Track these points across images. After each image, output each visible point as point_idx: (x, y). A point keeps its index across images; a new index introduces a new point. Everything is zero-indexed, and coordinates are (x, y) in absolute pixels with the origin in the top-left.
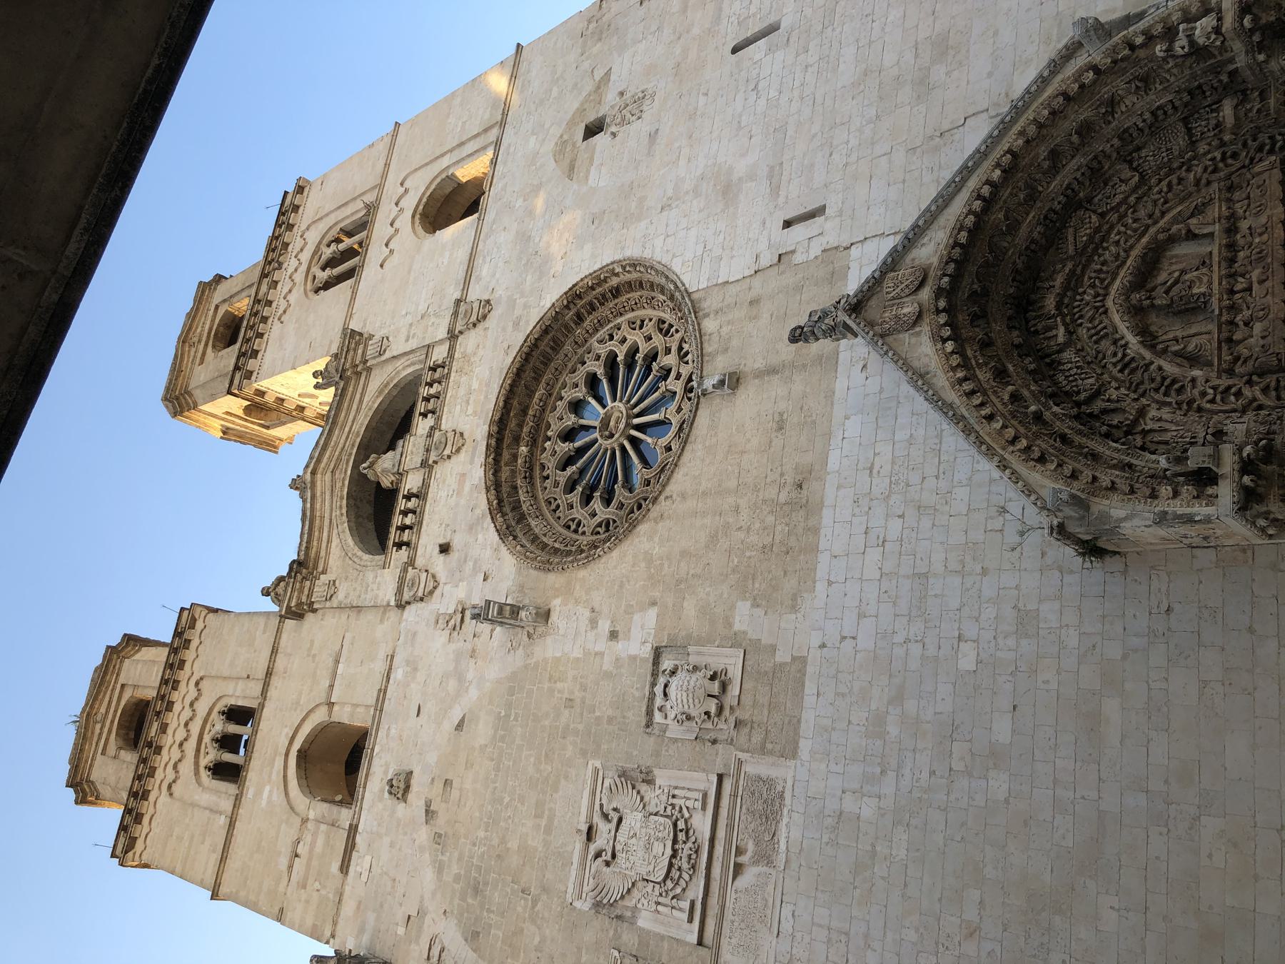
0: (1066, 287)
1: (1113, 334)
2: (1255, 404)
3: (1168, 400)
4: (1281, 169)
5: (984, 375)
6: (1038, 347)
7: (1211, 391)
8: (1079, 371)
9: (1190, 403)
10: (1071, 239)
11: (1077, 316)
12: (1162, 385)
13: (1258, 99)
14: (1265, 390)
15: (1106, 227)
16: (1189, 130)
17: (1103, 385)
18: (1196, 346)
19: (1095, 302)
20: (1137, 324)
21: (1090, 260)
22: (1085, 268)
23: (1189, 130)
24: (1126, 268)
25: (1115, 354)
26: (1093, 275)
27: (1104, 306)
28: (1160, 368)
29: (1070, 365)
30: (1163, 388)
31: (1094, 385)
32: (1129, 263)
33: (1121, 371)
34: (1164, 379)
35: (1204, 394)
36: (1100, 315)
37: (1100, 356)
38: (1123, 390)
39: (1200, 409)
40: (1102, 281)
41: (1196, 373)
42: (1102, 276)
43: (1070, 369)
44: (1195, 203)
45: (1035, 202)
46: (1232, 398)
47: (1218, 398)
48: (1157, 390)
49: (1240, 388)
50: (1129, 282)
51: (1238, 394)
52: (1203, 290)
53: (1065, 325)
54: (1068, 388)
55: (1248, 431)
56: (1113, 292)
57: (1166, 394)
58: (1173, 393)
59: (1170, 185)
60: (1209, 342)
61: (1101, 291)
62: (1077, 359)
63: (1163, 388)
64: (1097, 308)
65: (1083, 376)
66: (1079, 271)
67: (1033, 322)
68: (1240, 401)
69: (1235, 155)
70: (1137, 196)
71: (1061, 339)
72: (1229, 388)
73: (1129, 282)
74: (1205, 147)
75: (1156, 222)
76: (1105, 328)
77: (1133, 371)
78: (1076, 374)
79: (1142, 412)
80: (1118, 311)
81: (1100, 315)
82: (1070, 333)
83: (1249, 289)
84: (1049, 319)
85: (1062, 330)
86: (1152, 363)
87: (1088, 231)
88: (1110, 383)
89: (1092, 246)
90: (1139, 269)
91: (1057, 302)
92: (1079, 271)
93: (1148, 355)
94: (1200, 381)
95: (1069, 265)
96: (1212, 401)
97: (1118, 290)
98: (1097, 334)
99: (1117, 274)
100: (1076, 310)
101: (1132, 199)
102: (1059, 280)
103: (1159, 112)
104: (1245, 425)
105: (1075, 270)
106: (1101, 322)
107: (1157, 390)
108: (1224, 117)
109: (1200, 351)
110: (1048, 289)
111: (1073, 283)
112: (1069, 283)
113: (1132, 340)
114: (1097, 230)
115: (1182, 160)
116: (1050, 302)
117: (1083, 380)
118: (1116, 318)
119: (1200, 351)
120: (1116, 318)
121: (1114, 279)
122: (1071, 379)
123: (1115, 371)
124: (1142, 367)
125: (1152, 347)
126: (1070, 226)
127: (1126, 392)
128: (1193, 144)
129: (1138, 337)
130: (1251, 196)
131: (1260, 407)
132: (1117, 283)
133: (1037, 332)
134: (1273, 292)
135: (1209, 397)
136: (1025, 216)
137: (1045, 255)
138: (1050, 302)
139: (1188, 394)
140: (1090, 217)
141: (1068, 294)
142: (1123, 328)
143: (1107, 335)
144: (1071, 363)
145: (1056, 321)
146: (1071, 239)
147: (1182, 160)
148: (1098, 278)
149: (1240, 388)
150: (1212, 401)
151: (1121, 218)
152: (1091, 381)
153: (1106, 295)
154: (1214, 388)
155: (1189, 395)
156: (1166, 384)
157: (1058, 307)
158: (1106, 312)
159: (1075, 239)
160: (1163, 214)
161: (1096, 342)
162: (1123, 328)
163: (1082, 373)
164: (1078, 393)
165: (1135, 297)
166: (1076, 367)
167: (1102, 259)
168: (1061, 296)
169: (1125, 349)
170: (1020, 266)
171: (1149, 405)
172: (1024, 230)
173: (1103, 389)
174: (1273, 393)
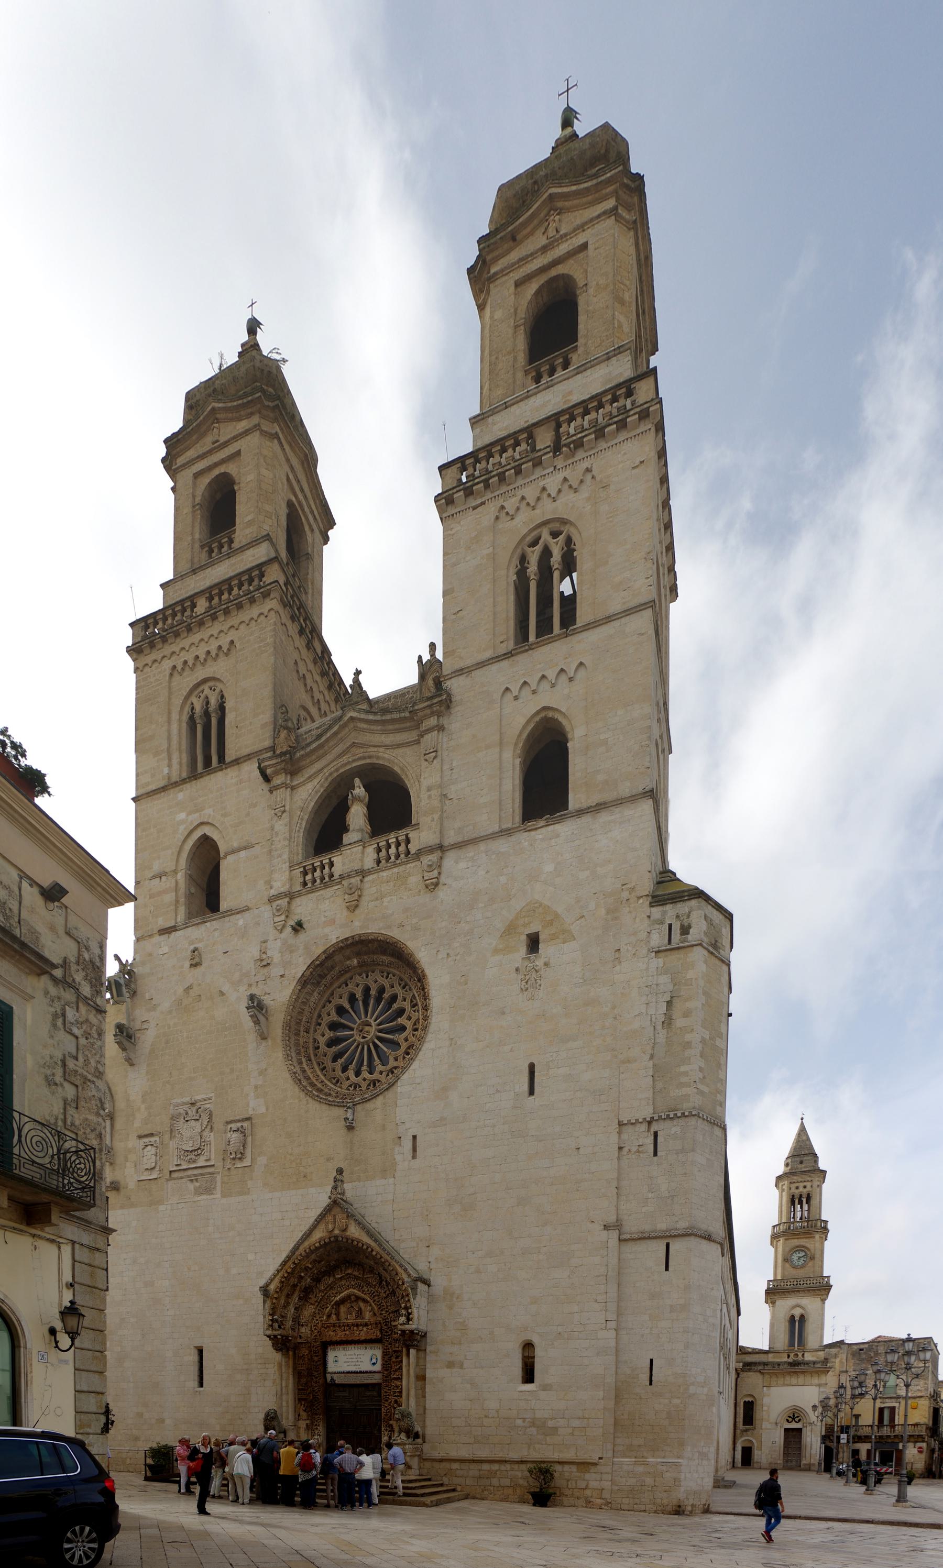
5: (313, 1257)
53: (343, 1277)
69: (386, 1325)
71: (337, 1276)
79: (311, 1304)
82: (341, 1278)
95: (361, 1276)
102: (356, 1273)
113: (338, 1298)
116: (349, 1271)
125: (335, 1304)
128: (392, 1312)
132: (356, 1292)
138: (349, 1271)
142: (342, 1295)
157: (348, 1274)
162: (342, 1295)
168: (351, 1274)
172: (368, 1261)
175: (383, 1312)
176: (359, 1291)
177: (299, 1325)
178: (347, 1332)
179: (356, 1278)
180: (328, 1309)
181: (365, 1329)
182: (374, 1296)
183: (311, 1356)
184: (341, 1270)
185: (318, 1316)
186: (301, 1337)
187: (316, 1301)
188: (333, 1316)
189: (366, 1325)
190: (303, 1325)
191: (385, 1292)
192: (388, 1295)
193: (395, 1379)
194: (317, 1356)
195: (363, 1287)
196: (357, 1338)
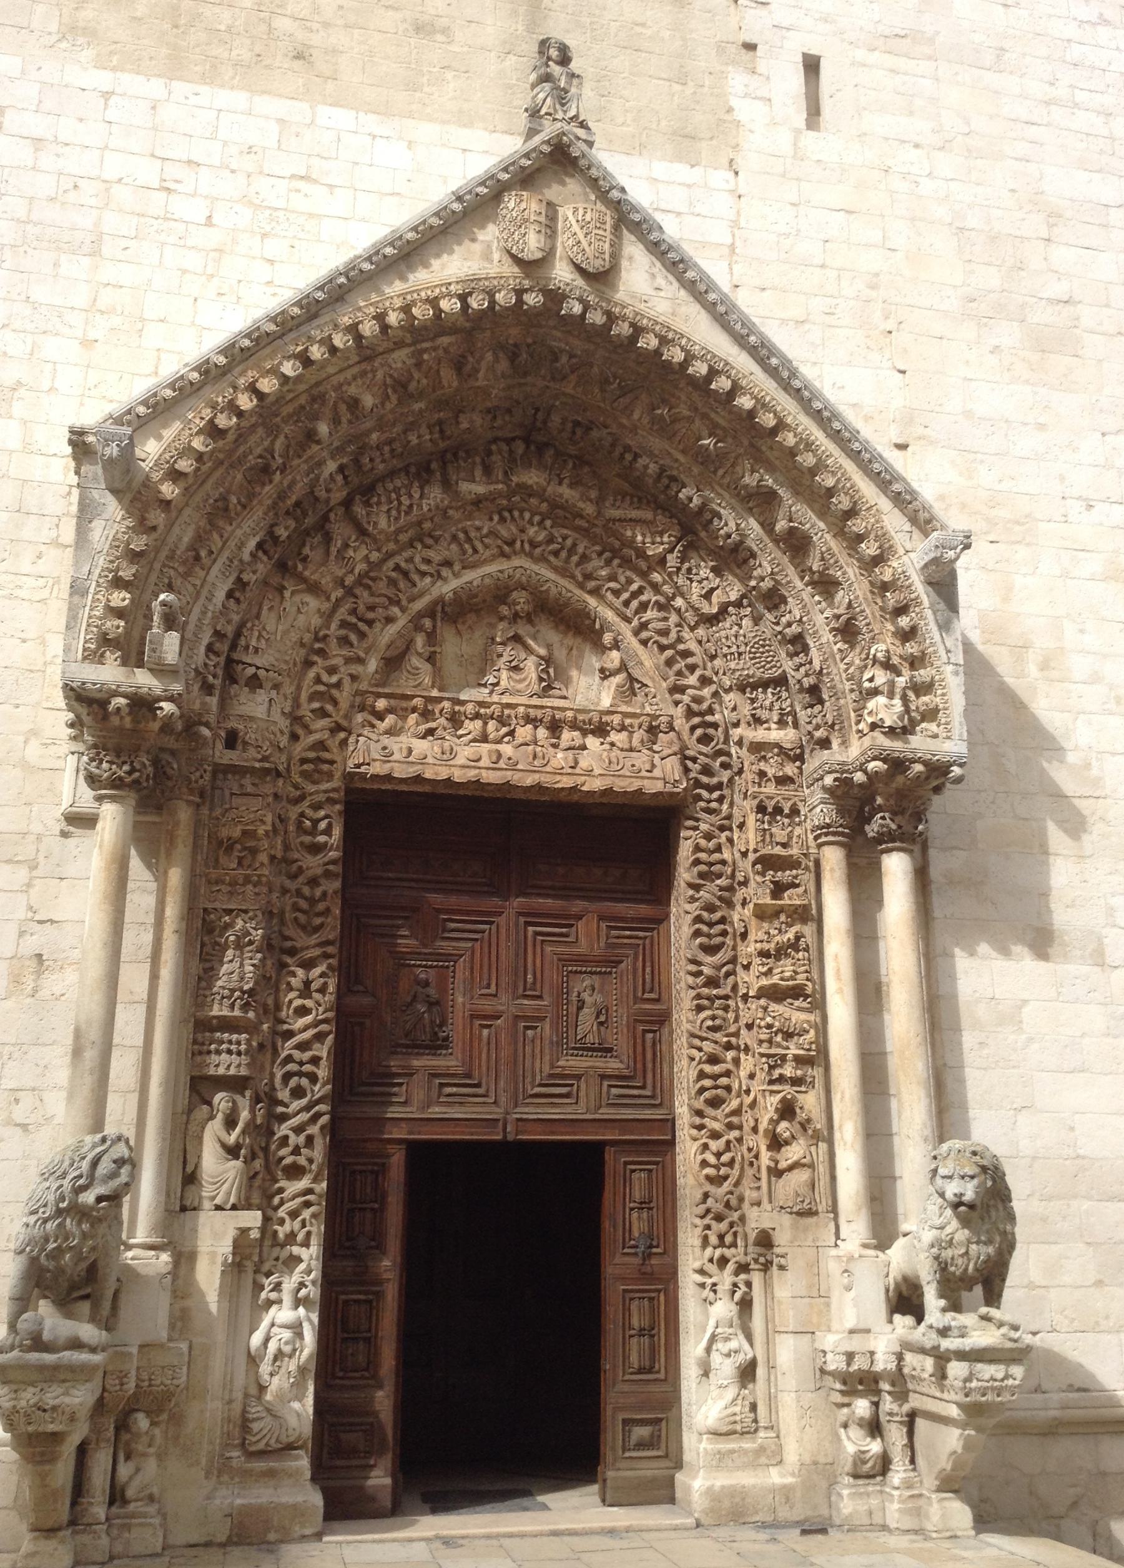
0: (555, 505)
1: (462, 561)
2: (300, 732)
3: (333, 626)
4: (661, 793)
6: (462, 454)
7: (334, 679)
8: (404, 508)
9: (321, 652)
10: (634, 514)
11: (506, 514)
12: (360, 619)
13: (781, 774)
14: (321, 745)
15: (643, 565)
16: (765, 684)
17: (375, 540)
18: (417, 669)
19: (522, 542)
20: (476, 596)
21: (594, 539)
22: (585, 532)
23: (765, 684)
24: (571, 587)
25: (428, 562)
26: (569, 542)
27: (515, 553)
28: (389, 620)
29: (417, 496)
30: (354, 620)
31: (374, 528)
32: (578, 592)
33: (397, 568)
34: (370, 623)
35: (332, 670)
36: (499, 547)
37: (430, 541)
38: (361, 567)
39: (308, 664)
40: (556, 554)
41: (373, 665)
42: (564, 554)
43: (411, 496)
44: (650, 684)
45: (702, 464)
46: (316, 705)
47: (322, 688)
48: (353, 612)
49: (330, 716)
50: (547, 591)
51: (322, 713)
52: (504, 683)
53: (491, 498)
54: (380, 490)
55: (252, 719)
56: (535, 568)
57: (344, 624)
58: (343, 632)
59: (687, 654)
60: (419, 684)
61: (538, 551)
62: (425, 508)
63: (354, 620)
64: (511, 543)
65: (394, 513)
66: (579, 522)
67: (505, 448)
68: (310, 714)
69: (705, 739)
70: (683, 609)
71: (465, 487)
72: (335, 703)
73: (547, 591)
74: (733, 703)
75: (636, 633)
76: (475, 551)
77: (392, 582)
78: (400, 503)
79: (314, 589)
80: (501, 571)
81: (499, 547)
82: (478, 502)
83: (484, 738)
84: (506, 473)
85: (480, 489)
86: (403, 610)
87: (639, 538)
88: (379, 550)
89: (617, 544)
90: (567, 604)
91: (531, 486)
92: (579, 522)
93: (419, 605)
94: (355, 669)
95: (589, 509)
96: (318, 680)
97: (537, 574)
98: (469, 540)
99: (563, 576)
100: (516, 514)
101: (679, 602)
102: (567, 492)
103: (799, 646)
104: (265, 717)
105: (582, 517)
106: (486, 547)
107: (353, 612)
108: (769, 729)
109: (409, 672)
110: (558, 475)
111: (560, 514)
112: (562, 508)
113: (448, 587)
114: (641, 553)
115: (721, 672)
116: (532, 477)
117: (389, 511)
118: (491, 569)
119: (409, 672)
120: (491, 569)
121: (555, 569)
122: (394, 496)
123: (399, 559)
124: (397, 596)
125: (430, 612)
126: (655, 516)
127: (357, 571)
128: (742, 688)
129: (451, 594)
130: (634, 754)
131: (295, 737)
132: (548, 574)
133: (489, 453)
134: (468, 767)
135: (325, 677)
136: (681, 447)
137: (618, 475)
139: (333, 648)
140: (662, 543)
141: (545, 505)
142: (471, 576)
143: (464, 552)
144: (421, 497)
145: (497, 482)
146: (634, 514)
147: (721, 672)
148: (562, 548)
149: (330, 716)
150: (318, 680)
151: (656, 588)
152: (383, 523)
153: (530, 555)
154: (338, 685)
155: (334, 653)
156: (360, 624)
158: (503, 554)
159: (631, 520)
160: (644, 643)
161: (454, 538)
162: (471, 576)
163: (399, 513)
164: (367, 504)
165: (521, 598)
166: (411, 506)
167: (594, 556)
168: (541, 495)
169: (432, 575)
170: (595, 434)
171: (328, 599)
173: (368, 540)
174: (312, 755)
175: (692, 680)
176: (563, 572)
177: (231, 677)
178: (507, 749)
179: (560, 514)
180: (392, 630)
181: (592, 742)
182: (644, 606)
183: (287, 847)
184: (488, 470)
185: (337, 655)
186: (232, 740)
187: (341, 582)
188: (415, 661)
189: (601, 731)
190: (255, 683)
191: (708, 596)
192: (723, 610)
193: (775, 994)
194: (316, 849)
195: (584, 558)
196: (566, 782)
